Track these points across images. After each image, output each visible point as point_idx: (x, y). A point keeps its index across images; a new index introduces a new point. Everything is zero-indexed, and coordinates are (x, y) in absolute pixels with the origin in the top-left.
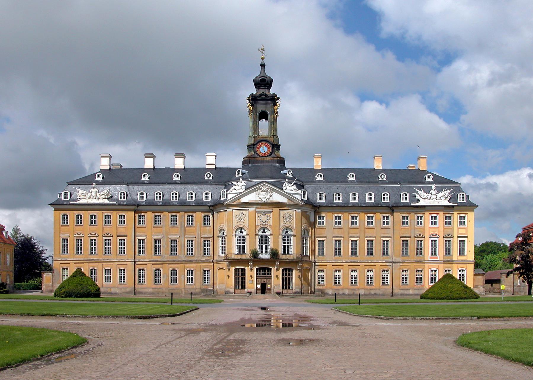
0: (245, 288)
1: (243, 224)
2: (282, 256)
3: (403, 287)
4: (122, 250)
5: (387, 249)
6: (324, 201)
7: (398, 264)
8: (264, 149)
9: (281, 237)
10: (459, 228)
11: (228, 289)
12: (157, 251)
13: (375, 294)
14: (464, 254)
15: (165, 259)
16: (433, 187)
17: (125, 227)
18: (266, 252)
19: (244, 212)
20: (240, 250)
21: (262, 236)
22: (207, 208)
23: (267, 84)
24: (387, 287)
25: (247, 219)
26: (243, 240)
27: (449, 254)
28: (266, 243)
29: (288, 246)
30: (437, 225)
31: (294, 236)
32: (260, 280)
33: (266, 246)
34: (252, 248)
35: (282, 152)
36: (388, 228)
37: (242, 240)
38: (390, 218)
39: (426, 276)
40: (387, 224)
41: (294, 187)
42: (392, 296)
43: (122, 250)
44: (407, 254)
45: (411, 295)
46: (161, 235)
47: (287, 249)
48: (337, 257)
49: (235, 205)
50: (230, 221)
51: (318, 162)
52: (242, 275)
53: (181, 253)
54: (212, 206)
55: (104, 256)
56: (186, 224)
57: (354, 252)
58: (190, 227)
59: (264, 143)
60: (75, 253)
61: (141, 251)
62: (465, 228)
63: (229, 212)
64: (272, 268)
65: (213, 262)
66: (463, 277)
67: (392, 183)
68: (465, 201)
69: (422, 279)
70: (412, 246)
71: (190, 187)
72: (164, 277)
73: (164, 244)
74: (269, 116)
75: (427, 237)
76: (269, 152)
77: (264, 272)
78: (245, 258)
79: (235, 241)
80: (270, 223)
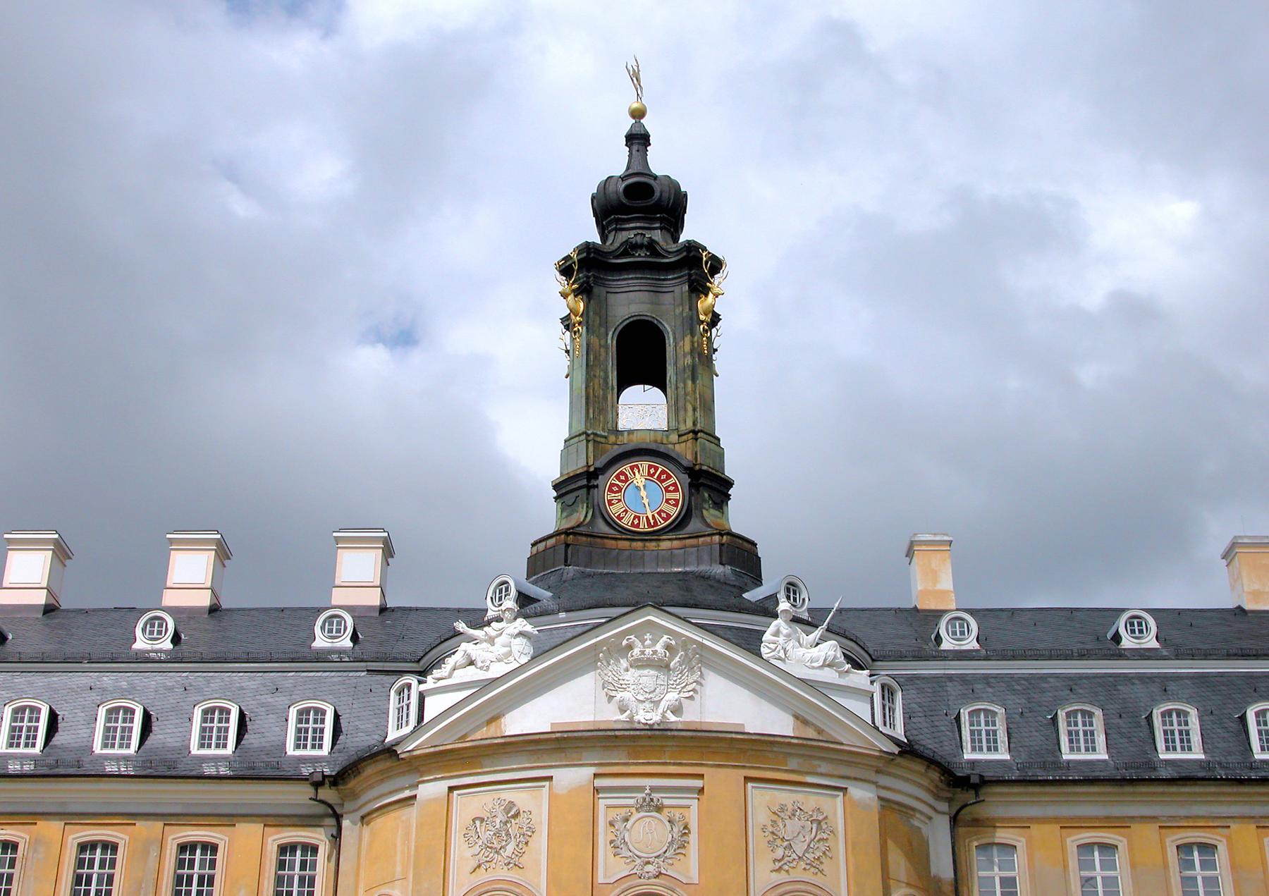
1: (513, 875)
22: (299, 796)
23: (659, 207)
25: (541, 842)
49: (465, 756)
51: (934, 575)
71: (218, 681)
74: (670, 341)
76: (674, 512)
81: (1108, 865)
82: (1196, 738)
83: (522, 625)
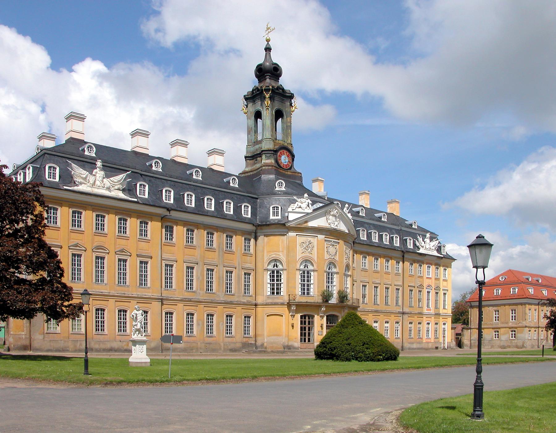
1: (310, 255)
11: (290, 344)
15: (201, 298)
16: (428, 235)
19: (310, 239)
21: (273, 272)
22: (249, 227)
24: (398, 340)
25: (315, 249)
29: (308, 285)
37: (306, 276)
45: (415, 349)
49: (301, 228)
50: (290, 249)
61: (169, 282)
63: (291, 237)
64: (316, 316)
78: (312, 301)
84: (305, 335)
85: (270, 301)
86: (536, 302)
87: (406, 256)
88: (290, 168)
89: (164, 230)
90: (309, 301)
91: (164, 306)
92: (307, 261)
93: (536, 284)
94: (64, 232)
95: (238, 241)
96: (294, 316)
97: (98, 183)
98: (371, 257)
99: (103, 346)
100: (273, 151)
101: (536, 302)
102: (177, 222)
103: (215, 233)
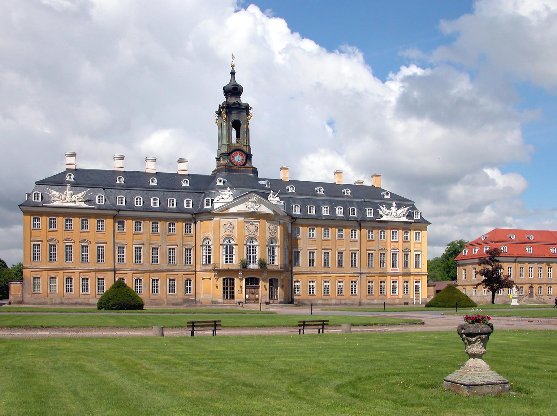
0: (233, 297)
2: (270, 267)
3: (369, 297)
4: (100, 258)
5: (355, 261)
6: (299, 213)
7: (364, 276)
8: (238, 158)
9: (245, 247)
10: (416, 243)
11: (215, 300)
12: (138, 259)
13: (345, 304)
14: (418, 268)
15: (146, 268)
16: (394, 204)
17: (104, 233)
18: (253, 262)
20: (227, 259)
22: (189, 216)
24: (356, 297)
26: (230, 250)
27: (407, 266)
28: (253, 253)
30: (397, 240)
31: (259, 245)
32: (248, 290)
33: (253, 256)
34: (242, 258)
35: (255, 162)
36: (356, 241)
37: (229, 250)
38: (358, 231)
39: (388, 286)
40: (355, 237)
41: (278, 199)
42: (360, 305)
43: (100, 258)
44: (372, 266)
45: (376, 304)
46: (142, 243)
47: (272, 259)
48: (312, 268)
49: (223, 214)
50: (217, 230)
52: (230, 285)
53: (162, 262)
54: (195, 214)
55: (65, 264)
56: (167, 231)
57: (326, 264)
58: (172, 235)
59: (238, 152)
60: (49, 260)
61: (121, 258)
62: (420, 243)
65: (195, 271)
66: (418, 288)
67: (357, 198)
68: (419, 218)
69: (385, 290)
70: (376, 257)
72: (145, 286)
73: (145, 252)
75: (389, 250)
76: (244, 162)
77: (252, 282)
78: (233, 268)
79: (222, 251)
80: (258, 234)
81: (313, 231)
82: (328, 212)
83: (231, 193)
84: (227, 293)
85: (204, 268)
86: (477, 261)
87: (362, 224)
88: (245, 164)
89: (116, 224)
90: (230, 268)
91: (116, 275)
92: (228, 238)
93: (509, 242)
94: (44, 232)
95: (179, 227)
96: (217, 279)
97: (67, 199)
98: (319, 228)
99: (70, 301)
100: (228, 153)
101: (513, 259)
102: (127, 218)
103: (159, 222)
